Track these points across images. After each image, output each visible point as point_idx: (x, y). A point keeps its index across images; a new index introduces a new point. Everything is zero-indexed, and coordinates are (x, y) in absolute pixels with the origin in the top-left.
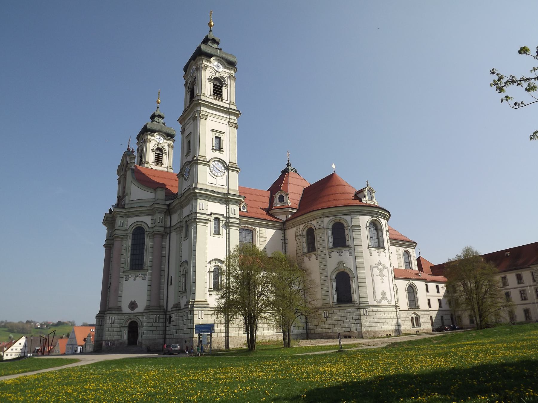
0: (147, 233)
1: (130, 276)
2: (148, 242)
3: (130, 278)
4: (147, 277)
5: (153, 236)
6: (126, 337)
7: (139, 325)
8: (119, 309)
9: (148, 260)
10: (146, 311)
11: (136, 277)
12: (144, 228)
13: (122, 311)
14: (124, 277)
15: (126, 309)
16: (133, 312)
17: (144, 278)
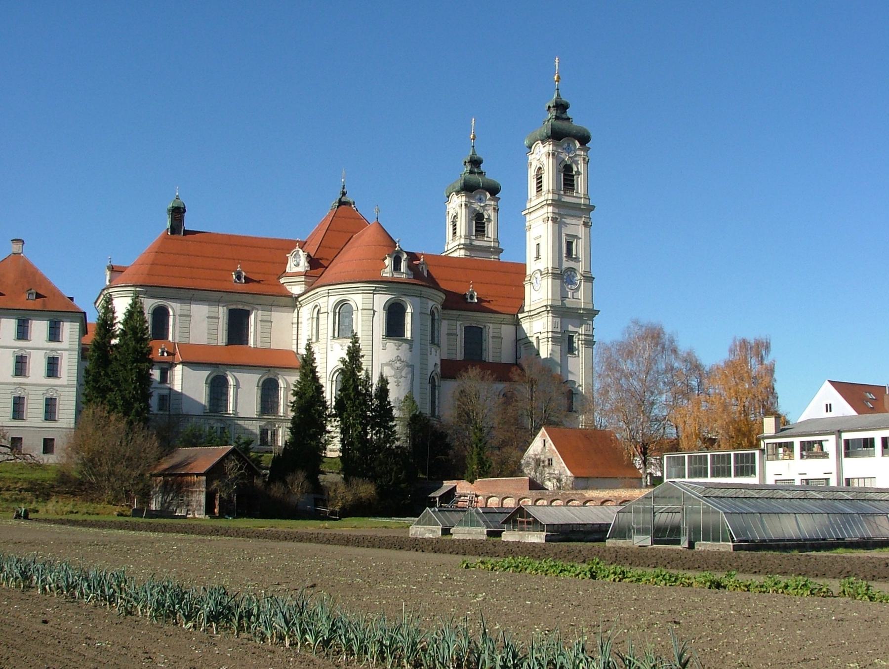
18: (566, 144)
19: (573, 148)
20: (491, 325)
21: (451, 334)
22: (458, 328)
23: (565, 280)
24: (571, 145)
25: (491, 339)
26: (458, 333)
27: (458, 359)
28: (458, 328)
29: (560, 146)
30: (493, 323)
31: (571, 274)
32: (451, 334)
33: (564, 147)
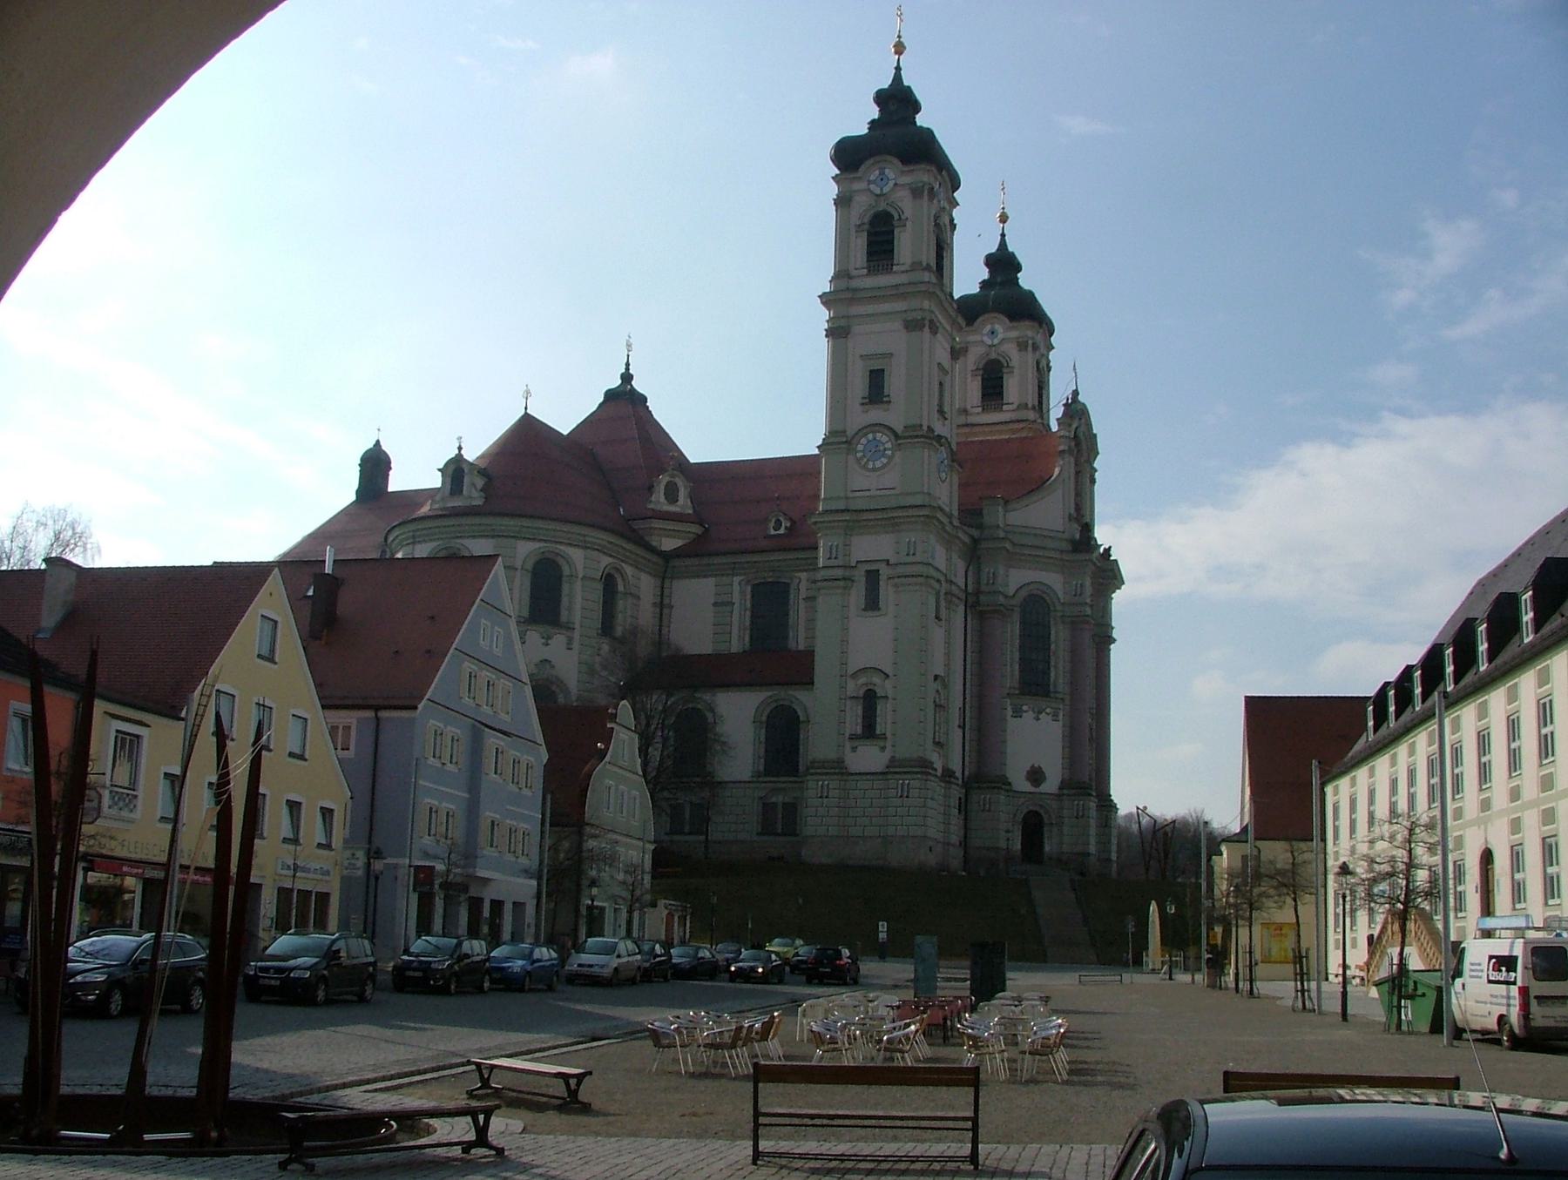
0: (1059, 614)
1: (1025, 708)
2: (1059, 636)
3: (1026, 712)
4: (1061, 717)
5: (1073, 623)
6: (1019, 847)
7: (1046, 820)
8: (1003, 783)
9: (1059, 676)
10: (1065, 792)
11: (1040, 712)
12: (1047, 598)
13: (1010, 784)
14: (1009, 708)
15: (1022, 784)
16: (1037, 790)
17: (1055, 717)
18: (877, 172)
19: (891, 176)
20: (803, 575)
21: (723, 604)
22: (736, 588)
23: (859, 455)
24: (887, 171)
25: (802, 605)
26: (736, 598)
27: (734, 650)
28: (736, 588)
29: (860, 178)
30: (806, 571)
31: (875, 439)
32: (723, 604)
33: (872, 178)
